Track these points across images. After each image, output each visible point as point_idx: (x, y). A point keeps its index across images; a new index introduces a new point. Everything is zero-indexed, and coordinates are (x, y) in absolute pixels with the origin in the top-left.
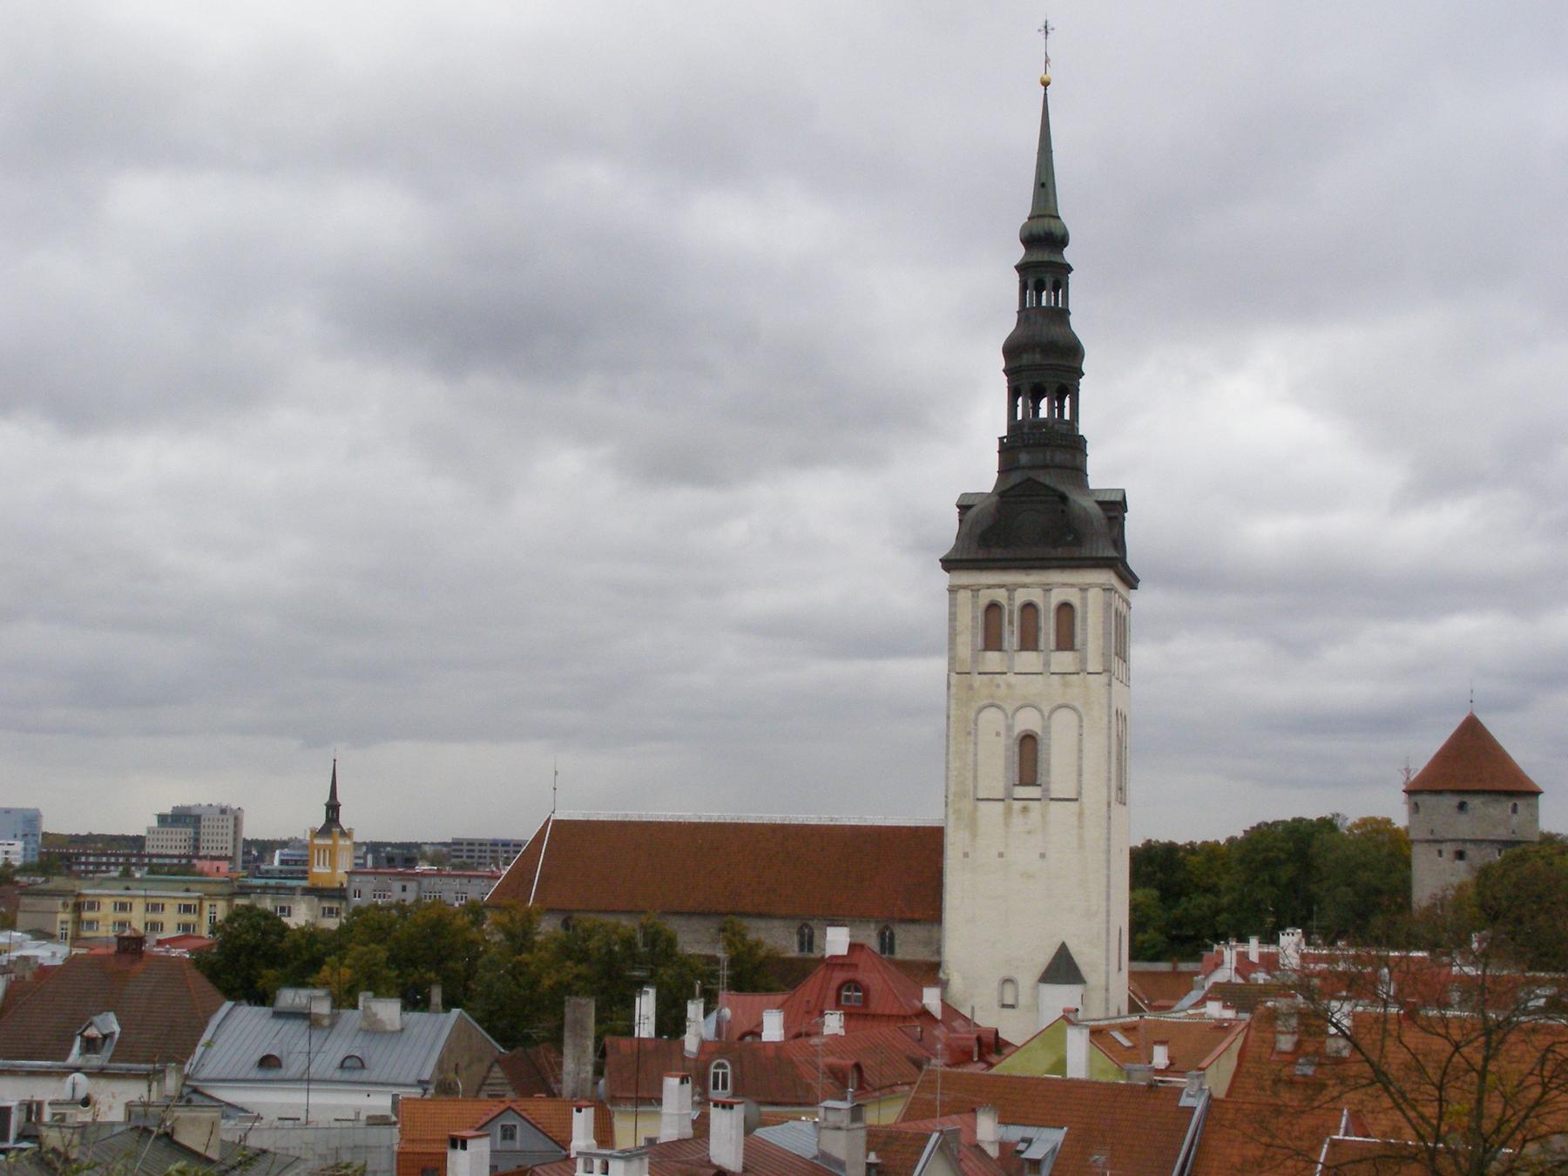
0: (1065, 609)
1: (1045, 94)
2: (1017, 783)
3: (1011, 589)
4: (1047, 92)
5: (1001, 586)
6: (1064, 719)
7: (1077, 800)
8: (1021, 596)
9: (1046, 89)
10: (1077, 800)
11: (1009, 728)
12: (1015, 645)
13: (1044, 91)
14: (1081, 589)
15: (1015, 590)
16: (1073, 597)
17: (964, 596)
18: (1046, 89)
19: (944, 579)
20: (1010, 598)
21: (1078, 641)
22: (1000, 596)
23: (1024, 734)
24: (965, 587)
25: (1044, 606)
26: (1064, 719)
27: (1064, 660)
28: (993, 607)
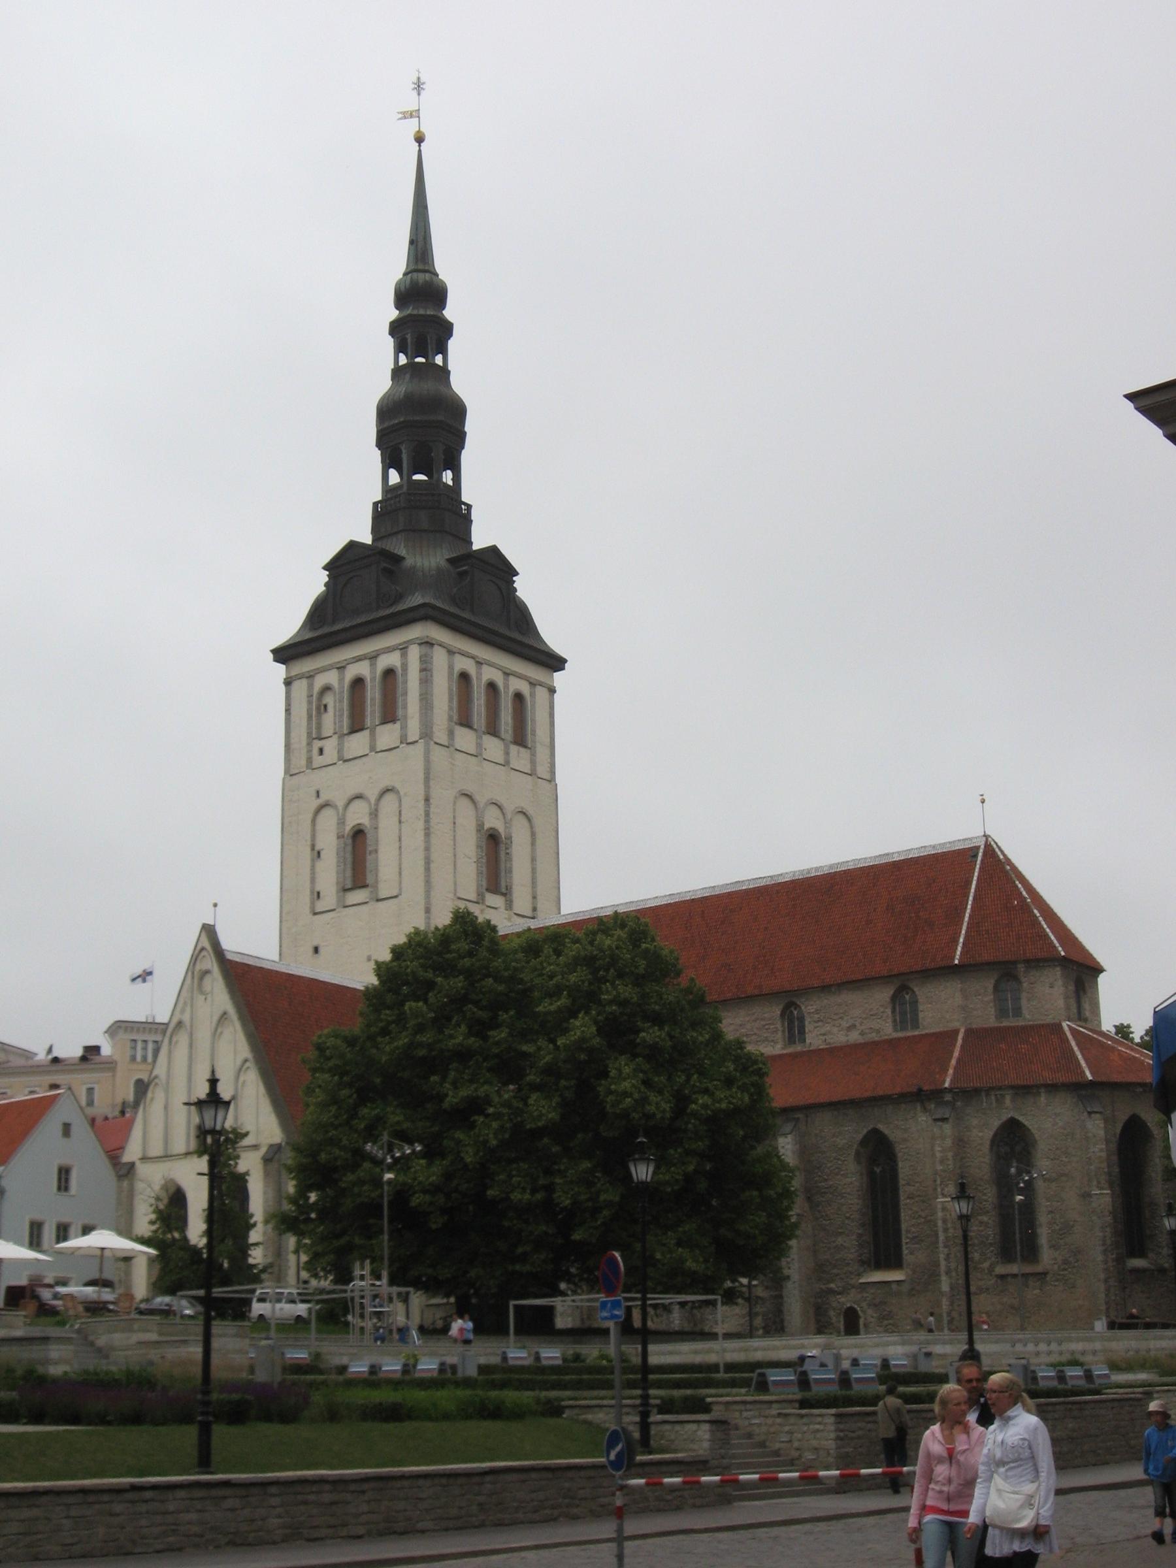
0: (389, 673)
1: (420, 151)
2: (349, 886)
3: (341, 668)
4: (422, 148)
6: (389, 802)
9: (420, 146)
11: (342, 822)
12: (345, 728)
13: (418, 148)
15: (344, 667)
16: (392, 660)
17: (300, 687)
18: (420, 146)
19: (281, 669)
21: (400, 712)
22: (331, 678)
23: (355, 829)
26: (389, 805)
27: (387, 735)
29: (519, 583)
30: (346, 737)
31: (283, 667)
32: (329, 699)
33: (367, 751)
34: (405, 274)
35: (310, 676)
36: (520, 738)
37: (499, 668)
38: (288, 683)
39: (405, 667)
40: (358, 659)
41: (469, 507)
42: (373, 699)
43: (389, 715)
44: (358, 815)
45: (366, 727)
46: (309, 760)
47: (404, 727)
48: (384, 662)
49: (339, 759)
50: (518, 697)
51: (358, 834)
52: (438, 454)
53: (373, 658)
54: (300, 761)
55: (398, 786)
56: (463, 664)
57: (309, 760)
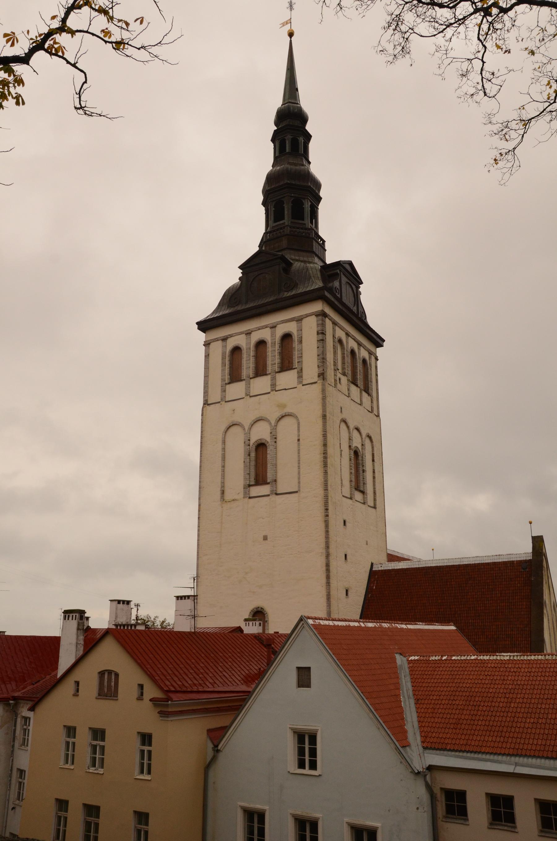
1: (291, 41)
3: (248, 333)
5: (241, 333)
6: (287, 425)
7: (296, 492)
8: (256, 337)
9: (291, 38)
10: (296, 492)
13: (290, 39)
14: (297, 321)
15: (250, 333)
17: (217, 347)
18: (291, 38)
22: (240, 341)
24: (216, 340)
25: (271, 340)
28: (237, 350)
29: (362, 288)
30: (252, 380)
31: (204, 334)
33: (269, 391)
34: (282, 105)
35: (224, 339)
36: (367, 389)
37: (355, 339)
38: (207, 344)
39: (300, 330)
41: (324, 242)
45: (267, 373)
47: (300, 371)
49: (247, 395)
50: (364, 361)
52: (307, 206)
53: (273, 327)
54: (215, 396)
56: (340, 334)
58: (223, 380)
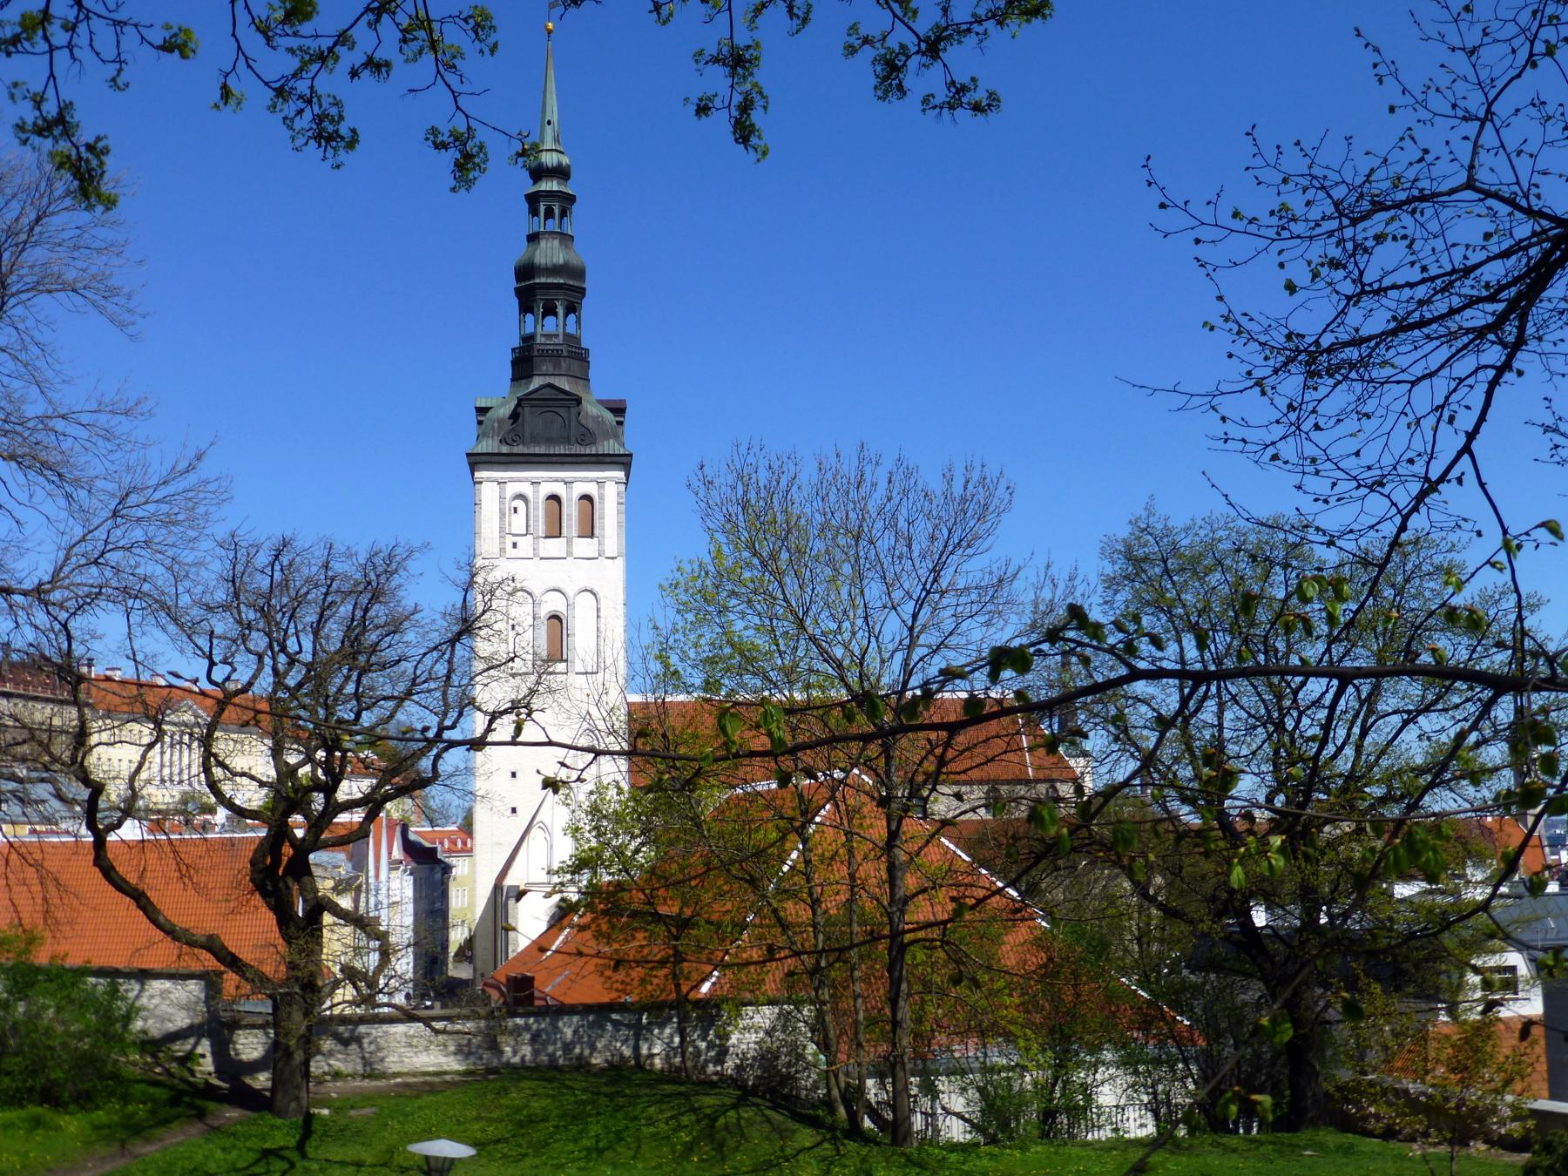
0: (586, 498)
8: (547, 489)
16: (591, 489)
20: (536, 492)
21: (597, 531)
22: (526, 489)
24: (489, 480)
27: (585, 546)
32: (520, 504)
39: (602, 497)
40: (556, 480)
42: (569, 515)
43: (589, 529)
44: (555, 603)
46: (503, 550)
48: (580, 489)
51: (555, 617)
55: (596, 589)
57: (503, 550)
58: (502, 529)
